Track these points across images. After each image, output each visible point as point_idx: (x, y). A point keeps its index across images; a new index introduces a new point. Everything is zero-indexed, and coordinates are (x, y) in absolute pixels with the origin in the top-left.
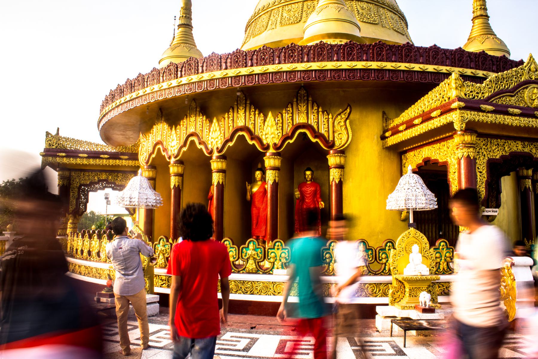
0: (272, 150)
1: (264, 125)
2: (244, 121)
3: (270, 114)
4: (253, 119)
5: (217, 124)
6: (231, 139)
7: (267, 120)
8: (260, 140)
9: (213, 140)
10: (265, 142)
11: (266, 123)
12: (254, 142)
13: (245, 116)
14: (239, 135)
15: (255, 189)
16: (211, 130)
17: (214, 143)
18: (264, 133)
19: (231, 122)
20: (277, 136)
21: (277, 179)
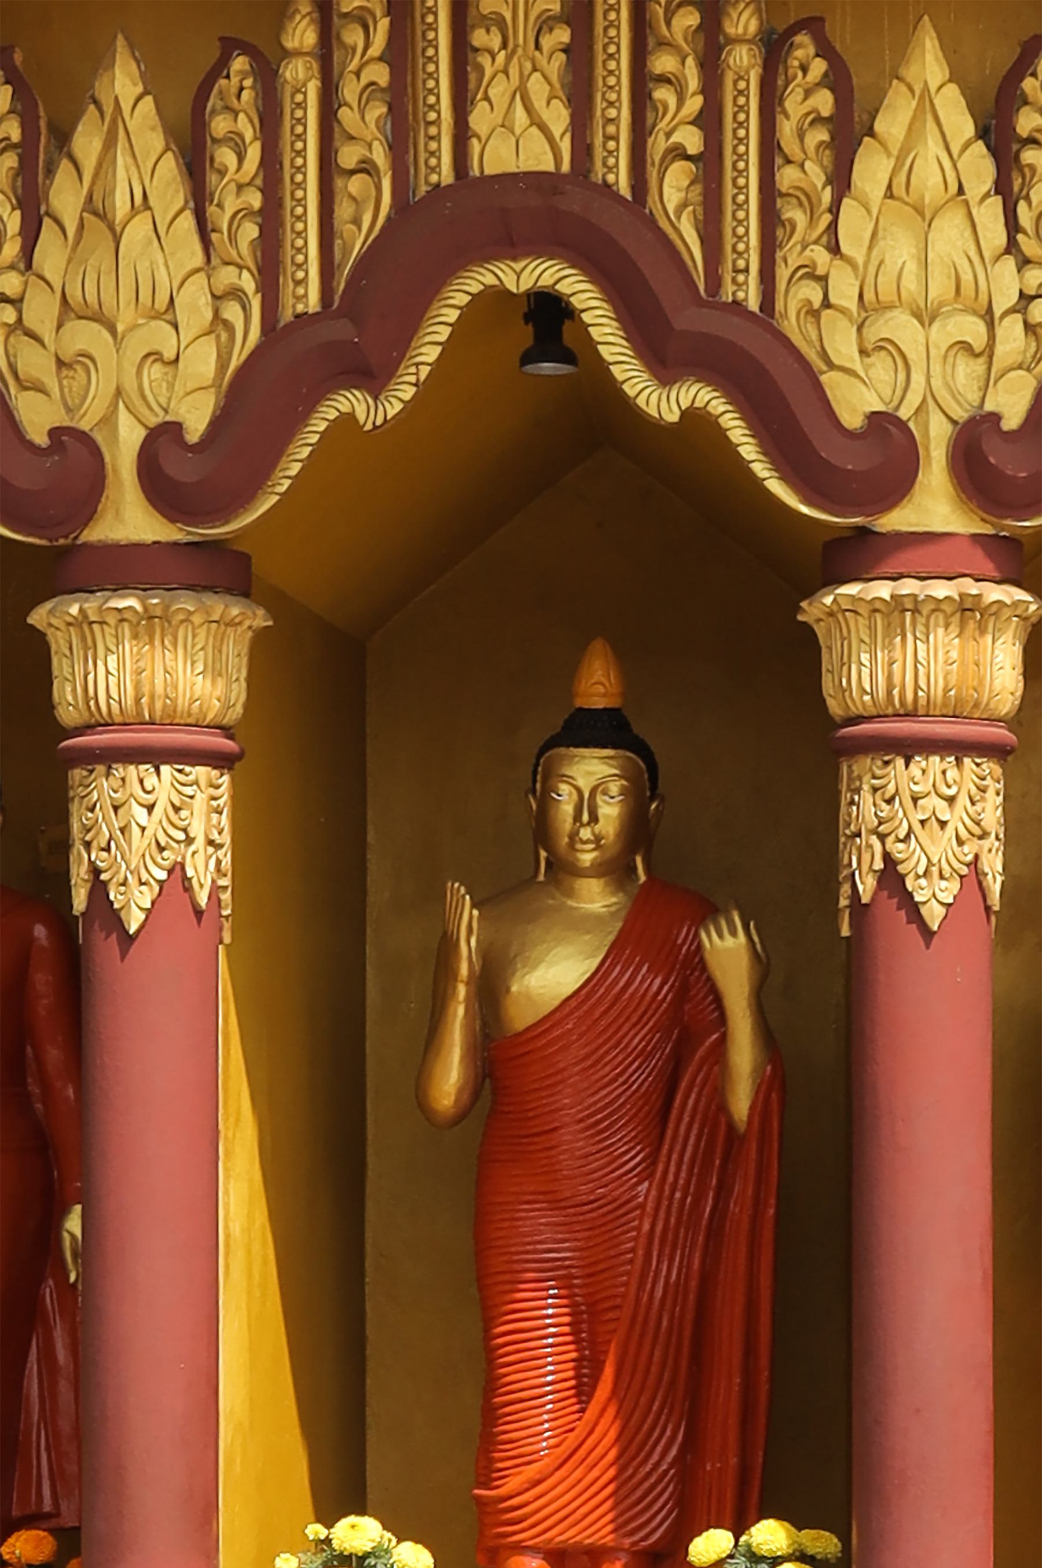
0: (933, 506)
1: (841, 180)
2: (558, 117)
3: (929, 64)
4: (694, 104)
5: (144, 125)
6: (354, 336)
7: (893, 122)
8: (776, 387)
9: (84, 336)
10: (854, 401)
11: (871, 170)
12: (697, 394)
13: (580, 58)
14: (495, 297)
15: (554, 974)
16: (65, 197)
17: (111, 365)
18: (844, 289)
19: (365, 123)
20: (1012, 337)
21: (993, 865)
